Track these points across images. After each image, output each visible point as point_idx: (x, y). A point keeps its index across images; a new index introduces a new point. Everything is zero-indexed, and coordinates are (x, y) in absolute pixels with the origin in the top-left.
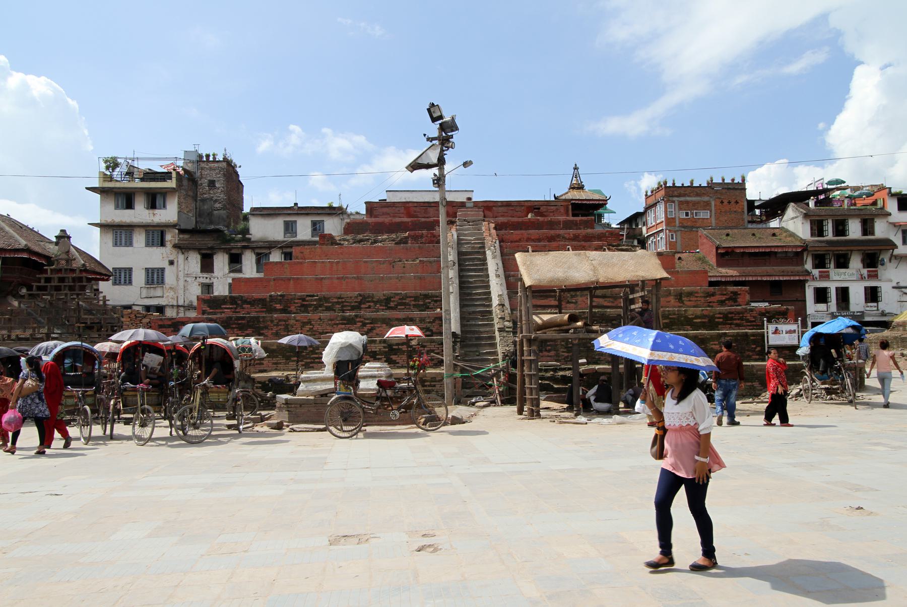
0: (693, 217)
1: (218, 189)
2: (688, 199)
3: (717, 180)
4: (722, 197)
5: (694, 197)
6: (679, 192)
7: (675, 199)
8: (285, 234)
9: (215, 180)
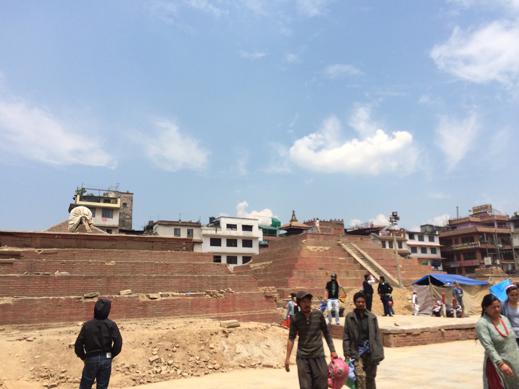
1: (128, 208)
3: (333, 219)
8: (175, 235)
9: (126, 203)
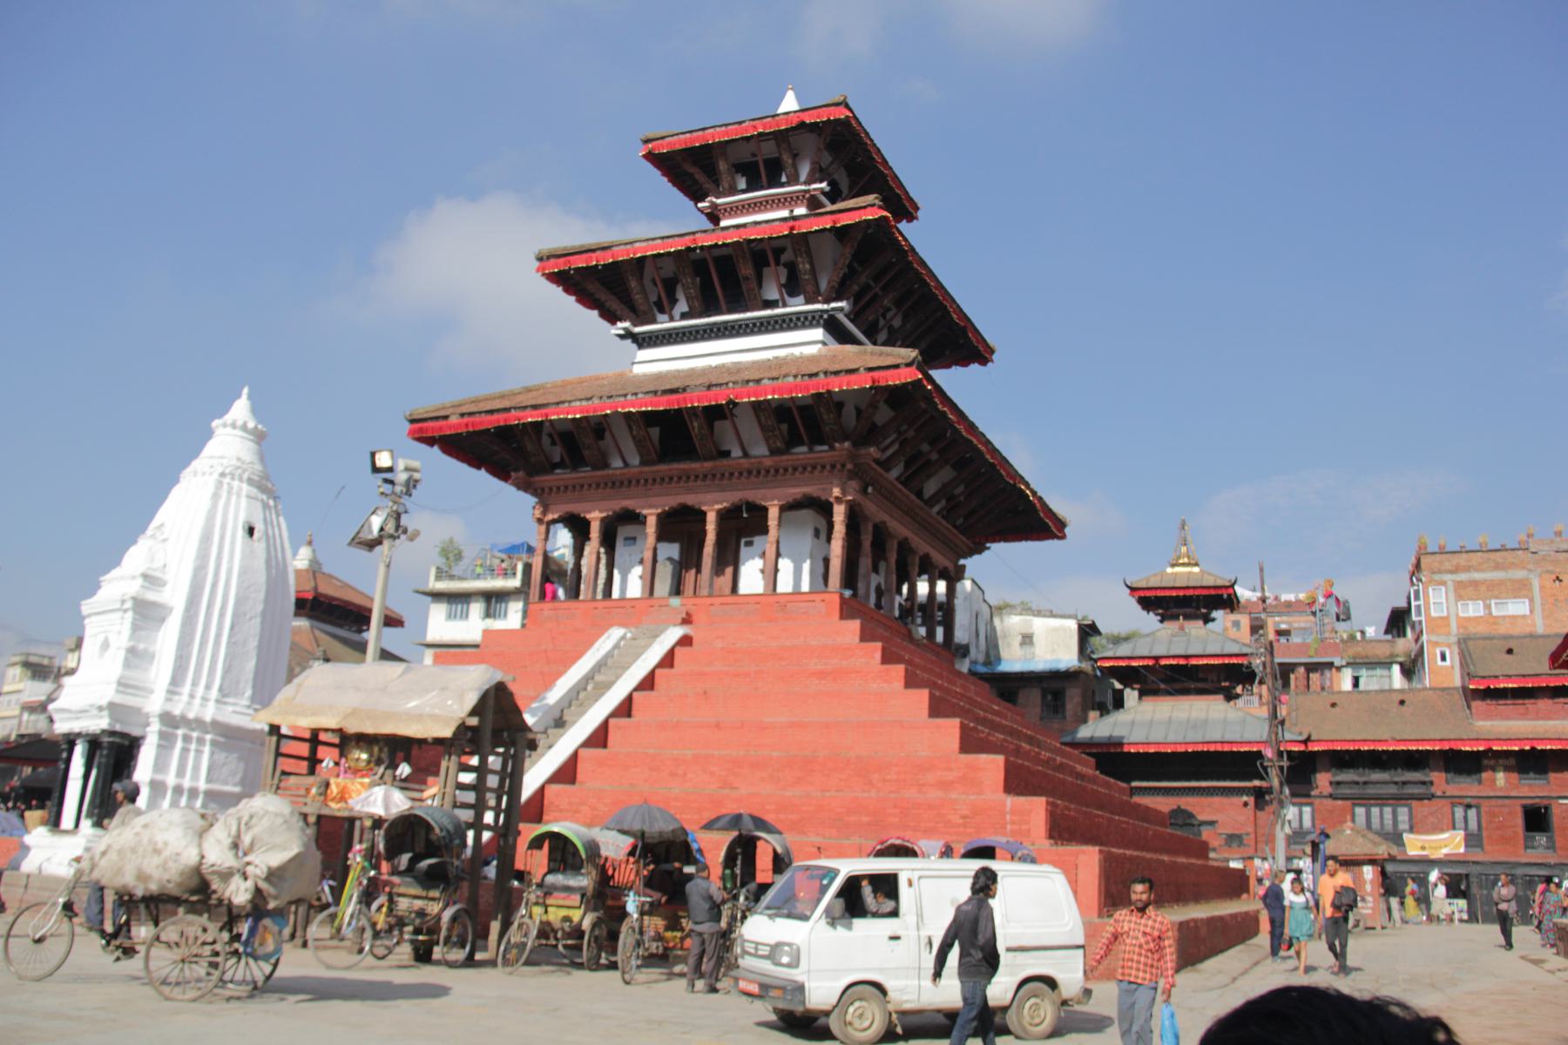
0: (1490, 613)
2: (1477, 576)
4: (1558, 570)
5: (1491, 571)
6: (1454, 563)
7: (1448, 577)
